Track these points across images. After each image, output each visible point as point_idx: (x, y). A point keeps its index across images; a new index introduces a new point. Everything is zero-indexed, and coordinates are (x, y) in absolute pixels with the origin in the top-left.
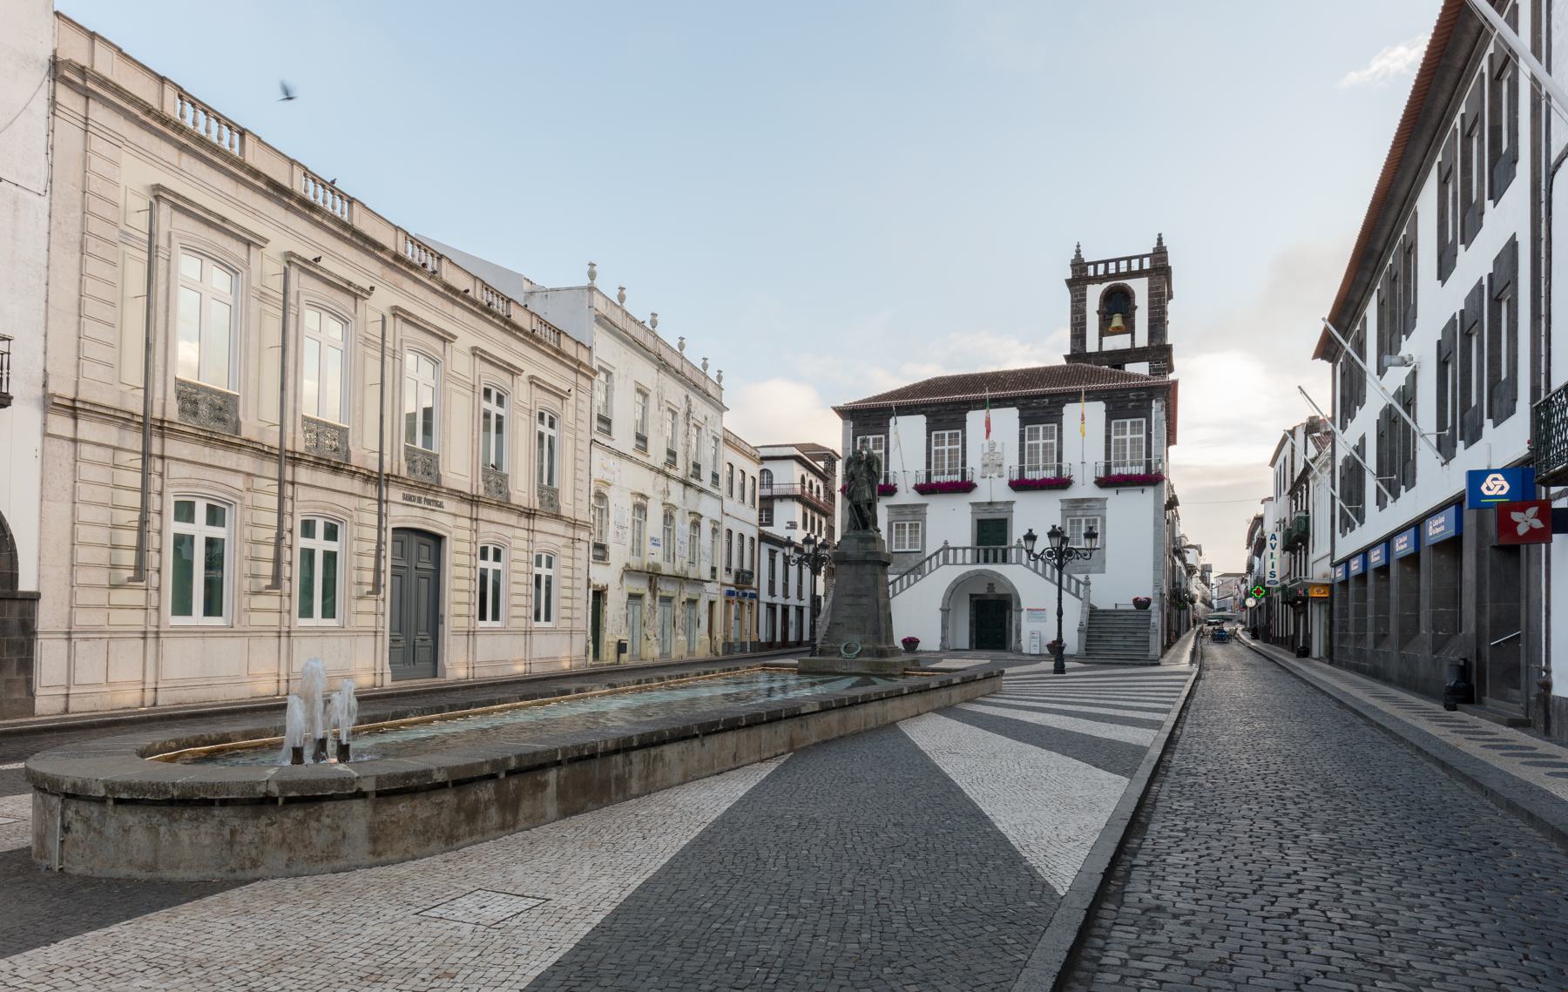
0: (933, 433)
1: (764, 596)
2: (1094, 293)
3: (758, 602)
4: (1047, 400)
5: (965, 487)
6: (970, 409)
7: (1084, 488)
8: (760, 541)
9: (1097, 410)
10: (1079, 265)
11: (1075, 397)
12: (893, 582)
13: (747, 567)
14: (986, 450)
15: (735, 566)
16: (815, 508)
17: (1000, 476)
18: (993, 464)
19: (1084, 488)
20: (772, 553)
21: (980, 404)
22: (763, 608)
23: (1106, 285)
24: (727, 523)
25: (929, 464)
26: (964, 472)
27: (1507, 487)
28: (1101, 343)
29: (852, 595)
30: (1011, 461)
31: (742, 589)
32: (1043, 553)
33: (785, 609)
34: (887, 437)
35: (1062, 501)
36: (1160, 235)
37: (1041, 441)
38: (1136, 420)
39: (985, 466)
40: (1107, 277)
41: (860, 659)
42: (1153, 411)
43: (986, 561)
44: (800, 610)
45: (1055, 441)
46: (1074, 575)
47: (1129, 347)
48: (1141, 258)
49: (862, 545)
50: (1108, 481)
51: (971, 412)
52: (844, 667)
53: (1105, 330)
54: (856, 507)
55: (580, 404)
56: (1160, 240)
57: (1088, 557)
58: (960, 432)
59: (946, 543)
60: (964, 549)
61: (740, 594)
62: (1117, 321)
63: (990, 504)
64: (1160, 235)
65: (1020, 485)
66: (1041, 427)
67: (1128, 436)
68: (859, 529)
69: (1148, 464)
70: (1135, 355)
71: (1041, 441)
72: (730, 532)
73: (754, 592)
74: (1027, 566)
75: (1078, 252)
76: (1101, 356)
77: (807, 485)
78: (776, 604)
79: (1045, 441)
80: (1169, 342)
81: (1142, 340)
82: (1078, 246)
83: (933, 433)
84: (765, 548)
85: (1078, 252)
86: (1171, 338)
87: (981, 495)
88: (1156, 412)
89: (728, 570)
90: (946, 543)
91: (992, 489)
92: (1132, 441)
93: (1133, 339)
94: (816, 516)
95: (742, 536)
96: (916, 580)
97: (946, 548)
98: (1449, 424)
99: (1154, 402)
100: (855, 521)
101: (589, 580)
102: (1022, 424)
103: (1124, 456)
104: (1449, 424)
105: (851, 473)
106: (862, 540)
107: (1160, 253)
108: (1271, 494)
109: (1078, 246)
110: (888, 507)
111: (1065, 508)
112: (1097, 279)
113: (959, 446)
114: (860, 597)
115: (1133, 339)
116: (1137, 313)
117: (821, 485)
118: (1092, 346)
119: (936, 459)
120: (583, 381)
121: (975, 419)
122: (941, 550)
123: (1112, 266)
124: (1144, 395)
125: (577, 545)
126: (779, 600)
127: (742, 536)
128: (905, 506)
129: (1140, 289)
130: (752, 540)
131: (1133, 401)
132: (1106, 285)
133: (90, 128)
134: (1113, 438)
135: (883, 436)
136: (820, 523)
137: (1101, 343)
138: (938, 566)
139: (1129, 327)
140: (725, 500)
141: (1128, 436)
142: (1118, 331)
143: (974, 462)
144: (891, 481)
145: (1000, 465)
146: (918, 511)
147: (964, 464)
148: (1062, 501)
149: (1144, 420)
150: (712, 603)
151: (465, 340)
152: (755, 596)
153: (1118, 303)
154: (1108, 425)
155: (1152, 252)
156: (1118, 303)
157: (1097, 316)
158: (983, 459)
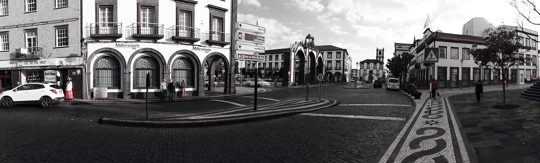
2: (378, 52)
5: (370, 69)
7: (378, 69)
9: (379, 64)
11: (378, 63)
18: (372, 67)
65: (374, 69)
70: (381, 57)
76: (379, 57)
81: (382, 56)
86: (384, 56)
91: (371, 69)
107: (383, 49)
118: (378, 56)
129: (382, 52)
139: (381, 55)
142: (380, 55)
143: (370, 67)
146: (366, 70)
153: (380, 52)
156: (380, 52)
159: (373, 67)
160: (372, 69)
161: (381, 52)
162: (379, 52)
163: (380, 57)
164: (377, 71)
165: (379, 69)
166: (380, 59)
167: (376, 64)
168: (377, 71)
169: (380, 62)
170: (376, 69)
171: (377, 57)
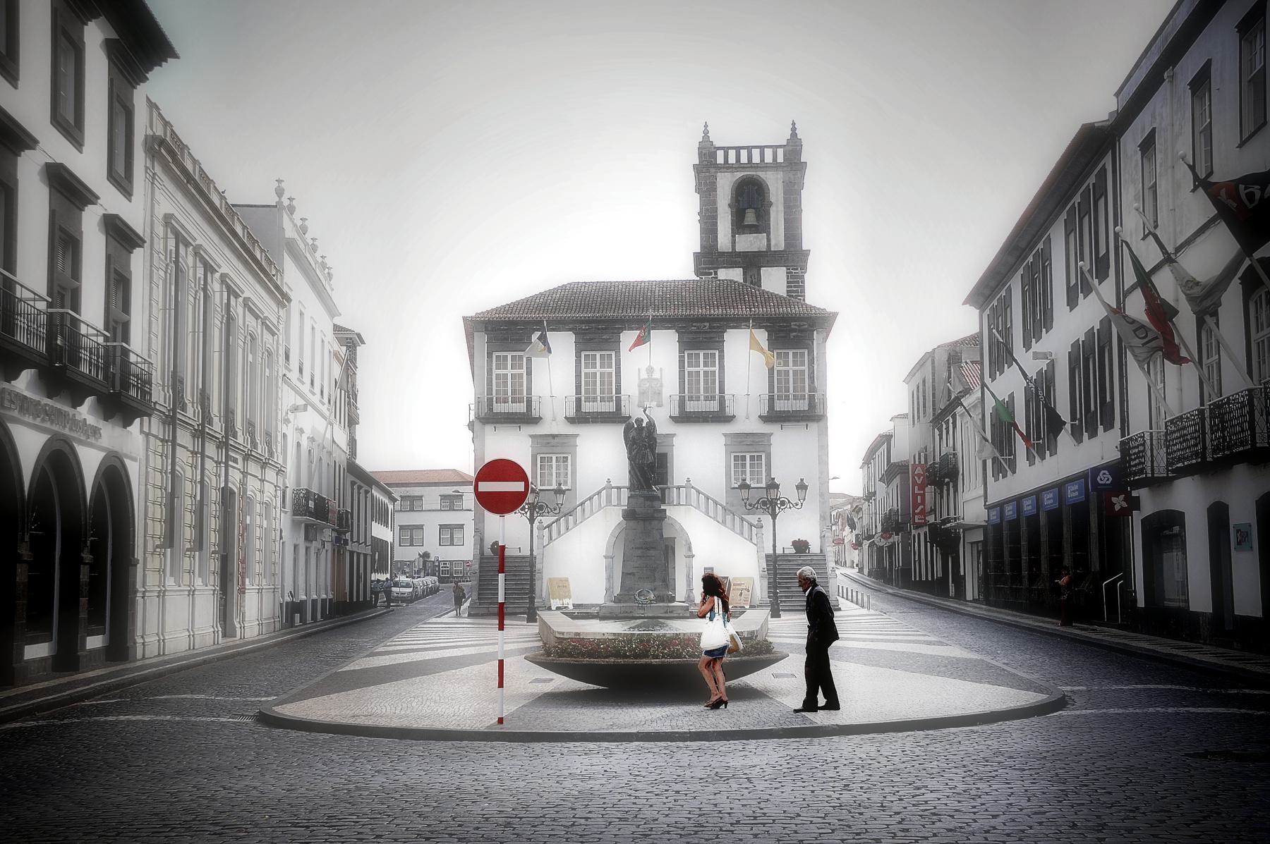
0: (583, 354)
2: (725, 185)
4: (707, 324)
7: (748, 422)
8: (348, 472)
12: (549, 526)
14: (644, 375)
17: (659, 406)
19: (748, 422)
20: (353, 483)
22: (348, 555)
23: (739, 175)
25: (578, 388)
26: (618, 400)
27: (1111, 479)
28: (734, 242)
29: (642, 548)
30: (671, 387)
32: (758, 502)
35: (725, 435)
36: (794, 124)
39: (643, 393)
40: (739, 166)
42: (815, 342)
45: (717, 369)
48: (775, 148)
49: (648, 503)
53: (739, 226)
56: (794, 129)
57: (799, 506)
59: (609, 481)
60: (619, 488)
62: (750, 218)
64: (794, 124)
71: (702, 369)
74: (698, 507)
75: (706, 133)
76: (733, 259)
79: (706, 369)
82: (706, 126)
83: (583, 354)
85: (706, 133)
90: (609, 481)
92: (795, 372)
93: (769, 240)
95: (340, 466)
96: (575, 524)
97: (609, 487)
98: (1078, 416)
99: (815, 332)
100: (639, 480)
102: (681, 351)
104: (1078, 416)
105: (633, 438)
106: (648, 498)
109: (706, 126)
110: (531, 436)
114: (648, 549)
116: (773, 211)
119: (587, 384)
122: (604, 488)
127: (340, 466)
128: (554, 436)
129: (774, 184)
133: (156, 182)
137: (734, 242)
138: (600, 508)
139: (761, 226)
140: (334, 425)
141: (791, 368)
142: (755, 229)
145: (660, 394)
148: (725, 435)
158: (639, 386)
163: (752, 263)
165: (767, 419)
166: (753, 279)
169: (771, 310)
170: (720, 417)
171: (709, 258)
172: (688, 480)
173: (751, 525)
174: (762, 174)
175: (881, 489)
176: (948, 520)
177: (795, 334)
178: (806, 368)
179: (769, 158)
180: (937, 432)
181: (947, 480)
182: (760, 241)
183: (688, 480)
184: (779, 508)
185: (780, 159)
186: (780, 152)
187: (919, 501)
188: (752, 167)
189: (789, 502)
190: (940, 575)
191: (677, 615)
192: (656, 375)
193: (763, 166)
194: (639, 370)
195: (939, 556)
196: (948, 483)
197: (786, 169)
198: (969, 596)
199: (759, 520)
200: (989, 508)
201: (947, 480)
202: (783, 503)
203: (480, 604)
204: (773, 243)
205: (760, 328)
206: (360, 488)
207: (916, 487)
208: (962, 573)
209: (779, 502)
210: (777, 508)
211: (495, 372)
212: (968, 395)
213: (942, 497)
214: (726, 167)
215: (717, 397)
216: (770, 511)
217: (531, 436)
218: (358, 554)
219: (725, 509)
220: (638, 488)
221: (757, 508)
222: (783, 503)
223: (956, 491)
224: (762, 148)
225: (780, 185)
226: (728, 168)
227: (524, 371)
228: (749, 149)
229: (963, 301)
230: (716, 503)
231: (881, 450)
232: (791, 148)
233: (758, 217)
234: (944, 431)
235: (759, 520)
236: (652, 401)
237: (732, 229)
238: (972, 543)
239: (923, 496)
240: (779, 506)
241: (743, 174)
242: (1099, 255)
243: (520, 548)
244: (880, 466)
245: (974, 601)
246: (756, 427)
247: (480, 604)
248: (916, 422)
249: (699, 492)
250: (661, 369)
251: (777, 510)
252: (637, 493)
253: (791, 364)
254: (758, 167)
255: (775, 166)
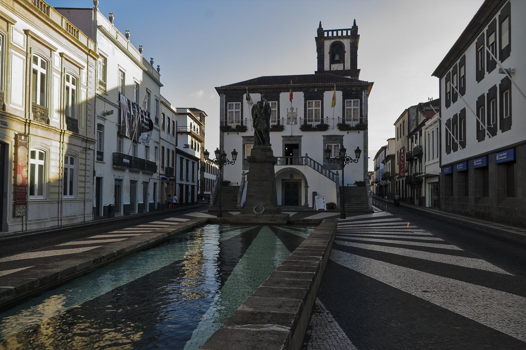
1: (178, 181)
2: (327, 44)
3: (176, 183)
6: (281, 92)
7: (334, 131)
9: (339, 94)
10: (320, 31)
11: (330, 89)
13: (170, 166)
14: (290, 111)
15: (166, 165)
16: (197, 139)
17: (296, 123)
18: (292, 118)
20: (182, 159)
21: (286, 90)
22: (177, 186)
23: (333, 41)
24: (162, 143)
31: (169, 177)
33: (187, 186)
34: (242, 104)
35: (323, 136)
36: (355, 20)
37: (314, 108)
38: (356, 100)
39: (289, 118)
40: (333, 37)
41: (265, 215)
42: (363, 96)
43: (291, 164)
44: (193, 187)
46: (331, 170)
47: (343, 69)
48: (347, 30)
50: (343, 127)
51: (282, 93)
52: (256, 220)
53: (333, 61)
54: (258, 132)
55: (89, 73)
58: (277, 102)
61: (168, 179)
62: (337, 58)
63: (291, 136)
66: (314, 101)
67: (352, 107)
68: (261, 144)
69: (361, 120)
70: (345, 72)
72: (163, 148)
73: (174, 178)
74: (310, 166)
75: (320, 25)
77: (193, 126)
78: (183, 184)
79: (316, 108)
80: (358, 68)
81: (348, 66)
82: (320, 23)
84: (178, 156)
85: (320, 25)
87: (287, 132)
88: (364, 97)
89: (163, 167)
92: (354, 109)
93: (344, 66)
94: (197, 142)
95: (168, 150)
99: (363, 92)
101: (94, 172)
102: (305, 100)
103: (351, 116)
107: (355, 29)
108: (394, 136)
109: (320, 23)
110: (243, 137)
111: (325, 139)
112: (328, 38)
113: (277, 109)
115: (344, 66)
117: (198, 127)
118: (327, 67)
120: (91, 60)
121: (284, 96)
123: (335, 33)
124: (359, 89)
125: (88, 152)
126: (184, 182)
127: (168, 150)
129: (347, 43)
130: (173, 152)
131: (354, 91)
132: (333, 41)
134: (346, 108)
135: (240, 103)
136: (198, 145)
139: (342, 61)
140: (161, 132)
144: (244, 124)
145: (296, 119)
147: (279, 117)
148: (323, 136)
149: (359, 100)
150: (155, 184)
151: (21, 24)
152: (174, 180)
154: (344, 102)
155: (351, 28)
157: (329, 55)
158: (288, 116)
159: (301, 114)
160: (297, 132)
161: (342, 46)
162: (333, 46)
164: (329, 139)
167: (321, 98)
168: (329, 139)
172: (307, 154)
173: (333, 174)
174: (342, 40)
175: (382, 166)
176: (417, 174)
177: (354, 92)
178: (359, 107)
179: (345, 33)
180: (410, 140)
181: (415, 158)
182: (341, 66)
183: (307, 154)
184: (346, 162)
185: (349, 34)
186: (349, 32)
187: (402, 167)
188: (338, 38)
189: (351, 159)
190: (410, 196)
191: (278, 222)
192: (294, 111)
193: (342, 37)
194: (287, 109)
195: (410, 188)
196: (416, 159)
197: (351, 38)
198: (427, 205)
199: (337, 172)
200: (442, 167)
201: (415, 158)
202: (348, 160)
203: (214, 206)
204: (346, 67)
205: (339, 90)
206: (187, 161)
207: (401, 162)
208: (424, 195)
209: (346, 159)
210: (345, 162)
211: (228, 110)
212: (430, 119)
213: (412, 165)
214: (328, 38)
215: (320, 120)
216: (341, 164)
217: (243, 137)
218: (187, 186)
219: (322, 167)
220: (258, 144)
221: (334, 162)
222: (348, 160)
223: (421, 162)
224: (342, 30)
225: (349, 45)
226: (328, 38)
227: (240, 110)
228: (337, 31)
229: (433, 72)
230: (318, 164)
231: (382, 153)
232: (353, 30)
233: (340, 58)
234: (414, 139)
235: (337, 172)
236: (292, 122)
237: (330, 62)
238: (429, 183)
239: (404, 165)
240: (346, 161)
241: (334, 40)
242: (501, 48)
243: (237, 183)
244: (382, 157)
245: (429, 208)
246: (336, 132)
247: (214, 206)
248: (399, 138)
249: (311, 159)
250: (297, 109)
251: (345, 164)
252: (257, 147)
253: (353, 105)
254: (340, 38)
255: (347, 37)
